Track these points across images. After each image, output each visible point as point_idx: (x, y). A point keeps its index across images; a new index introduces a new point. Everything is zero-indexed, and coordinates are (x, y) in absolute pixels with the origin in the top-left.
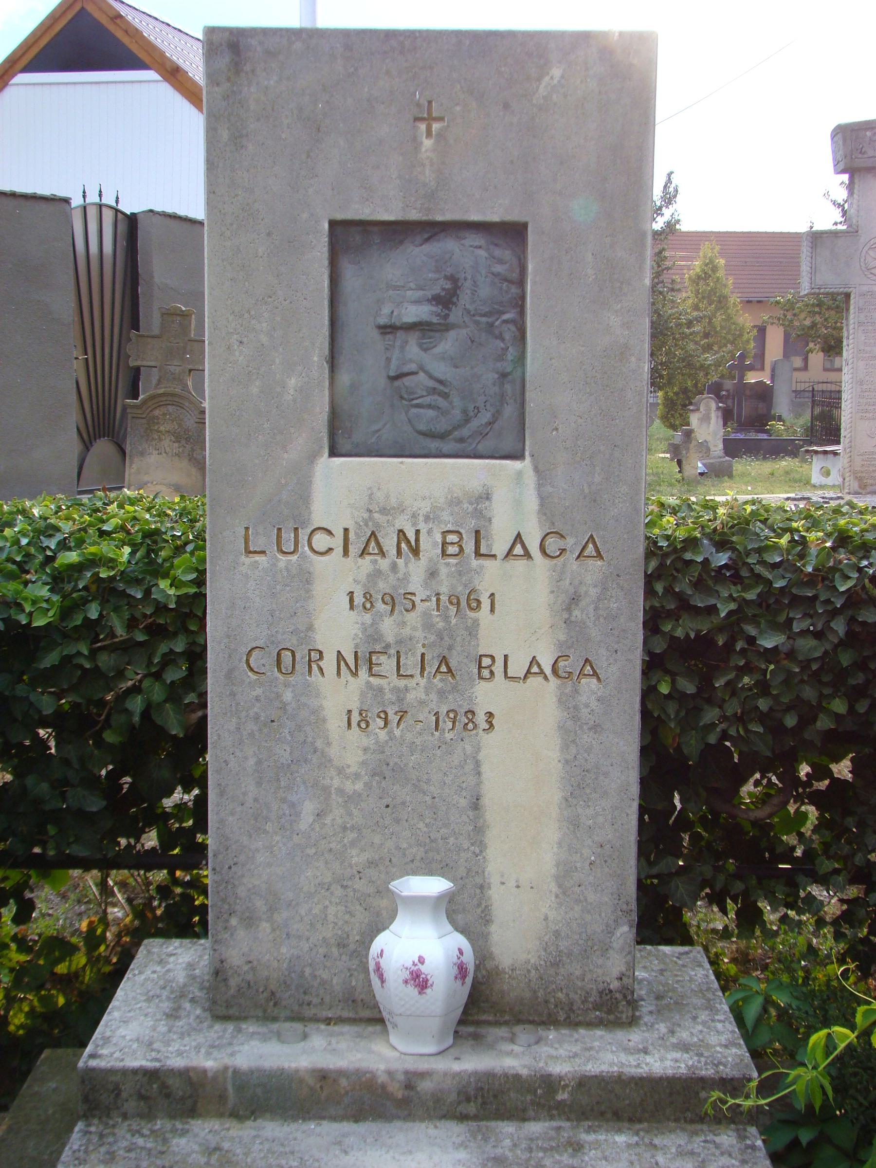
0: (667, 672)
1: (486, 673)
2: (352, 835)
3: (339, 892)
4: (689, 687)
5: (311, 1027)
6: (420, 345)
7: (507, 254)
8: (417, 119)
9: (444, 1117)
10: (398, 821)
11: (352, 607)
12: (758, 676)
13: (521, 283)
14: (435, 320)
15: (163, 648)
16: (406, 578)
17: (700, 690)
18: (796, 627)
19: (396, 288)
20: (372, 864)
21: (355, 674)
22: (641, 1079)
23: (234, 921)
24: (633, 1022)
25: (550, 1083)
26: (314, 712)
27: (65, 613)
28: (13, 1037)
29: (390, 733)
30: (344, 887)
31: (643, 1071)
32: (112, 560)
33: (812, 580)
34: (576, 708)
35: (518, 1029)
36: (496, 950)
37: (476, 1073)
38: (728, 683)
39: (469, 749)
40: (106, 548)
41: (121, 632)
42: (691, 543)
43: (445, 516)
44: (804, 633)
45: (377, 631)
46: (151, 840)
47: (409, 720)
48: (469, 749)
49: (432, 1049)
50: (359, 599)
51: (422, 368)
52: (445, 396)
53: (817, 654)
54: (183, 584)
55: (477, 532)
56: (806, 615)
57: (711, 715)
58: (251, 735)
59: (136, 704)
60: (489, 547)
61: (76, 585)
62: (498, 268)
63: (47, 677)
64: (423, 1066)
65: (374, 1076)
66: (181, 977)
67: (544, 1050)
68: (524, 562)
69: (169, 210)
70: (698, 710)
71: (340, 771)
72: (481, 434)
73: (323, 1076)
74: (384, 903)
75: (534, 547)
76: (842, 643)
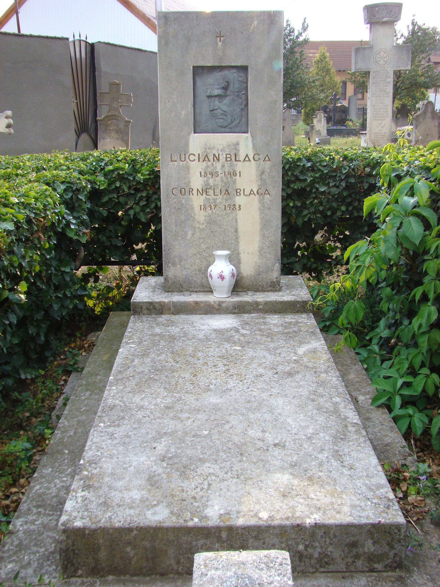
0: (292, 200)
1: (238, 194)
2: (202, 240)
3: (199, 256)
4: (299, 204)
5: (192, 293)
6: (219, 101)
7: (242, 74)
8: (217, 37)
9: (229, 313)
10: (215, 236)
11: (201, 176)
12: (319, 200)
13: (247, 83)
15: (139, 195)
16: (216, 168)
17: (302, 204)
18: (331, 185)
19: (212, 85)
20: (208, 248)
21: (202, 195)
22: (282, 302)
23: (170, 265)
24: (280, 290)
25: (257, 304)
26: (191, 206)
27: (109, 185)
28: (97, 316)
29: (212, 211)
30: (200, 255)
31: (282, 300)
32: (123, 168)
33: (335, 171)
34: (264, 203)
35: (249, 292)
36: (242, 271)
38: (310, 203)
39: (234, 215)
40: (121, 165)
41: (126, 190)
42: (299, 159)
43: (227, 150)
44: (332, 186)
46: (134, 257)
47: (217, 207)
48: (234, 215)
49: (226, 296)
50: (203, 174)
51: (219, 108)
52: (226, 115)
53: (337, 193)
54: (145, 175)
55: (235, 154)
56: (334, 181)
57: (305, 212)
58: (174, 213)
59: (132, 212)
60: (239, 158)
61: (112, 176)
62: (240, 79)
63: (104, 205)
66: (154, 284)
67: (256, 296)
68: (248, 162)
69: (106, 41)
70: (302, 211)
71: (198, 222)
73: (196, 303)
74: (211, 259)
75: (251, 159)
76: (344, 189)
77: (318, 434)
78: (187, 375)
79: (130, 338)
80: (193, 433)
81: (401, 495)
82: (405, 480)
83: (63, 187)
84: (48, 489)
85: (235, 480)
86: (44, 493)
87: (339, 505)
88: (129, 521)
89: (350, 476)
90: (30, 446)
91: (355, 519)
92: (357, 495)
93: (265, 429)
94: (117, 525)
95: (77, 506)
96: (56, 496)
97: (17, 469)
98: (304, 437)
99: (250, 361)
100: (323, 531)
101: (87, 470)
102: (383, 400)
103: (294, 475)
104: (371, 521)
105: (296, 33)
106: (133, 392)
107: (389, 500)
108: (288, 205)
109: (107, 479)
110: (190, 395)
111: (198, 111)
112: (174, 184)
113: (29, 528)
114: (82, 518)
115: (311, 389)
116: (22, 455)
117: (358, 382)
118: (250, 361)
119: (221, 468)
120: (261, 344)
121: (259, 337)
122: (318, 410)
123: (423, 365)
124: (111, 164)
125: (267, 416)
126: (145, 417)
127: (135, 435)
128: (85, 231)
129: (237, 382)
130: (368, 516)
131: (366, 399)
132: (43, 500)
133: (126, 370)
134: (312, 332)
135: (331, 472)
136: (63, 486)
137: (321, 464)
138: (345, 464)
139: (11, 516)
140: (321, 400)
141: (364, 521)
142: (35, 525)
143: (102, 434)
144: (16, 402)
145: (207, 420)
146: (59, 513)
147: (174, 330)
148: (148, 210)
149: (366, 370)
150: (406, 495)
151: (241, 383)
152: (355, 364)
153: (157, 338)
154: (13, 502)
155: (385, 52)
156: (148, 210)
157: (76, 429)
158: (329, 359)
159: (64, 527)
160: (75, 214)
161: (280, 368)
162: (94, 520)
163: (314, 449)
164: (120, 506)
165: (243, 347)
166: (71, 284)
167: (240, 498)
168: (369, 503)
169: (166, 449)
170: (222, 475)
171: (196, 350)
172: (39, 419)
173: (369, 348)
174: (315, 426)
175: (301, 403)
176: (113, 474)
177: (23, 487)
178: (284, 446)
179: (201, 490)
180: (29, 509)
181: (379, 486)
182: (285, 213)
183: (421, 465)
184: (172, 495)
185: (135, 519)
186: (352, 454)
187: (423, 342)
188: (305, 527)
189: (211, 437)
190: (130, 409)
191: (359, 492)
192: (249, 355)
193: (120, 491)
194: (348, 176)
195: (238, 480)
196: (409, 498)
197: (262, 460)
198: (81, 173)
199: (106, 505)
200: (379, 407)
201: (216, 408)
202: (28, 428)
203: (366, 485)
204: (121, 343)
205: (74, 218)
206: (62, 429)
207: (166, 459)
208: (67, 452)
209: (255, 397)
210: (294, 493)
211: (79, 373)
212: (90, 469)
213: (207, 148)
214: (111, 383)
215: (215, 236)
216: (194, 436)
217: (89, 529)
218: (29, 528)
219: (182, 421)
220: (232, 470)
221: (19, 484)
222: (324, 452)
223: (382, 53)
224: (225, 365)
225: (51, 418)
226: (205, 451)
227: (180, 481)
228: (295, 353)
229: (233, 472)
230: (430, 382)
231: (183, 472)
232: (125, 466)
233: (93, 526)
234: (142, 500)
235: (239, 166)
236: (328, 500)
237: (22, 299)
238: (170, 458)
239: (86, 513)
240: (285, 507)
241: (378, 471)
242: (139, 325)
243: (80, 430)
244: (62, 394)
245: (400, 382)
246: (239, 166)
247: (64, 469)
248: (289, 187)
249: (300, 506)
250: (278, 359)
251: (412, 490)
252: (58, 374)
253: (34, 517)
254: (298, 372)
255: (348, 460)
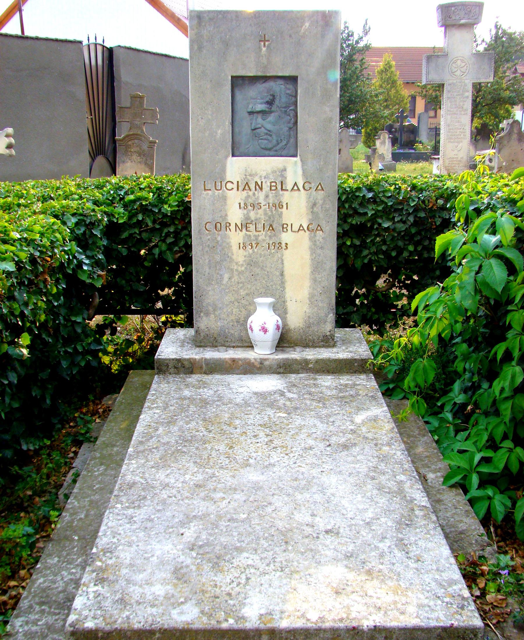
0: (350, 237)
1: (285, 230)
3: (237, 304)
4: (358, 243)
5: (228, 349)
9: (273, 373)
10: (256, 280)
11: (240, 208)
12: (382, 238)
13: (296, 97)
14: (267, 110)
15: (166, 231)
16: (258, 197)
17: (361, 242)
18: (396, 220)
20: (248, 294)
21: (241, 231)
23: (202, 314)
24: (334, 346)
25: (306, 362)
26: (228, 244)
27: (130, 218)
29: (253, 250)
30: (239, 302)
31: (337, 357)
32: (146, 198)
33: (401, 203)
34: (315, 241)
35: (296, 347)
37: (283, 359)
38: (371, 241)
39: (279, 256)
40: (144, 194)
41: (150, 224)
42: (358, 189)
43: (271, 177)
44: (398, 222)
45: (249, 216)
47: (259, 246)
48: (279, 256)
49: (269, 353)
50: (242, 205)
51: (262, 126)
52: (271, 136)
53: (403, 229)
54: (173, 206)
56: (400, 215)
57: (365, 252)
58: (207, 252)
59: (156, 251)
60: (286, 187)
61: (133, 207)
63: (123, 242)
64: (266, 357)
65: (250, 360)
66: (182, 337)
67: (305, 353)
68: (297, 192)
70: (361, 251)
71: (237, 263)
72: (283, 149)
73: (234, 360)
74: (252, 308)
75: (301, 188)
76: (412, 225)
77: (378, 519)
78: (222, 448)
79: (154, 402)
80: (228, 516)
81: (478, 593)
82: (483, 574)
83: (74, 220)
84: (54, 582)
85: (279, 574)
86: (49, 588)
87: (403, 604)
88: (150, 622)
89: (417, 569)
90: (33, 531)
91: (422, 621)
92: (426, 593)
93: (315, 512)
94: (136, 626)
95: (89, 603)
96: (63, 591)
97: (17, 559)
98: (361, 523)
99: (297, 431)
100: (384, 635)
101: (101, 560)
102: (457, 479)
103: (350, 568)
104: (441, 624)
105: (356, 37)
106: (157, 467)
107: (463, 598)
108: (344, 243)
109: (124, 571)
110: (226, 471)
111: (237, 130)
112: (208, 217)
113: (30, 629)
114: (94, 618)
115: (371, 464)
116: (23, 541)
117: (427, 457)
118: (297, 431)
119: (261, 559)
120: (311, 410)
121: (308, 402)
122: (379, 490)
123: (505, 437)
124: (133, 193)
125: (318, 497)
126: (171, 497)
127: (158, 518)
128: (100, 273)
129: (282, 455)
130: (438, 617)
131: (436, 477)
132: (47, 596)
133: (148, 440)
134: (372, 396)
135: (393, 564)
136: (72, 580)
137: (382, 555)
138: (411, 555)
139: (8, 615)
140: (383, 478)
141: (433, 624)
142: (37, 625)
143: (119, 518)
144: (17, 478)
145: (245, 501)
146: (66, 611)
147: (207, 393)
148: (176, 248)
149: (437, 442)
150: (484, 593)
151: (287, 457)
152: (424, 436)
153: (186, 402)
154: (11, 598)
155: (462, 61)
156: (176, 248)
157: (88, 511)
158: (393, 428)
159: (72, 629)
160: (89, 253)
161: (334, 440)
162: (108, 620)
163: (373, 537)
164: (140, 603)
165: (289, 414)
166: (83, 336)
167: (284, 595)
168: (439, 602)
169: (195, 535)
170: (262, 567)
171: (232, 417)
172: (44, 499)
173: (440, 416)
174: (375, 509)
175: (358, 482)
176: (131, 565)
177: (23, 580)
178: (338, 533)
179: (237, 586)
180: (31, 607)
181: (452, 582)
182: (341, 253)
183: (502, 557)
184: (203, 591)
185: (159, 620)
186: (420, 543)
187: (506, 409)
188: (362, 630)
189: (250, 521)
190: (152, 487)
191: (428, 588)
192: (297, 423)
193: (141, 586)
194: (416, 209)
195: (282, 573)
196: (488, 597)
197: (312, 550)
198: (96, 203)
199: (123, 602)
200: (452, 486)
201: (257, 487)
202: (29, 509)
203: (436, 580)
204: (142, 408)
205: (88, 257)
206: (71, 511)
207: (195, 547)
208: (76, 538)
209: (303, 473)
210: (349, 589)
211: (92, 444)
212: (104, 559)
213: (248, 174)
214: (130, 455)
215: (256, 280)
216: (229, 520)
217: (102, 631)
218: (30, 629)
219: (215, 502)
220: (274, 562)
221: (19, 576)
222: (386, 540)
223: (459, 62)
224: (267, 435)
225: (58, 498)
226: (243, 539)
227: (212, 574)
228: (352, 421)
229: (276, 564)
230: (513, 458)
231: (216, 563)
232: (146, 555)
233: (108, 628)
234: (167, 597)
235: (286, 197)
236: (390, 598)
237: (24, 355)
238: (201, 547)
239: (99, 612)
240: (338, 606)
241: (451, 564)
242: (164, 386)
243: (92, 512)
244: (71, 468)
245: (477, 457)
246: (286, 197)
247: (73, 559)
248: (345, 222)
249: (356, 604)
250: (331, 428)
251: (492, 587)
252: (67, 445)
253: (37, 617)
254: (355, 445)
255: (414, 551)
